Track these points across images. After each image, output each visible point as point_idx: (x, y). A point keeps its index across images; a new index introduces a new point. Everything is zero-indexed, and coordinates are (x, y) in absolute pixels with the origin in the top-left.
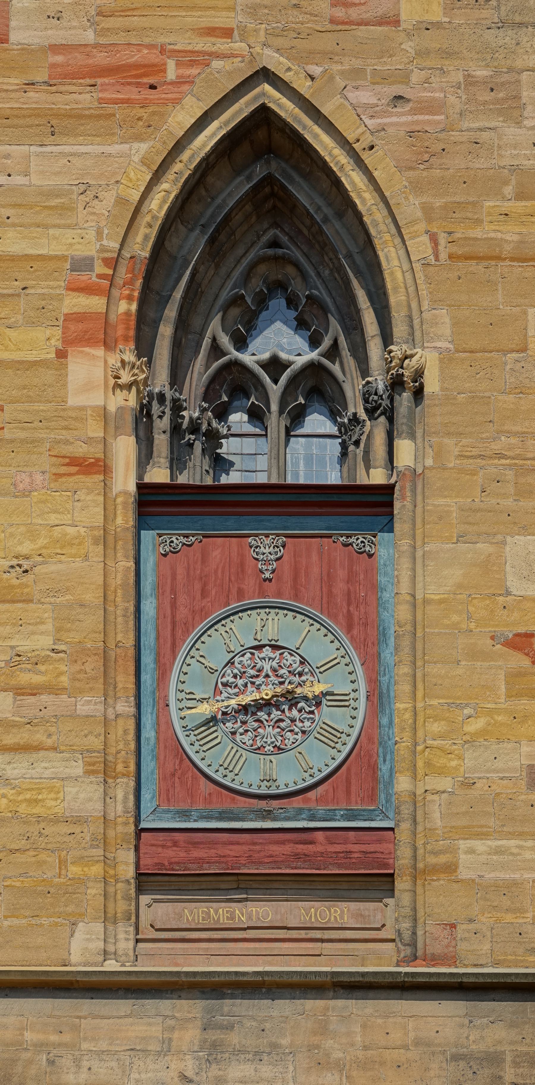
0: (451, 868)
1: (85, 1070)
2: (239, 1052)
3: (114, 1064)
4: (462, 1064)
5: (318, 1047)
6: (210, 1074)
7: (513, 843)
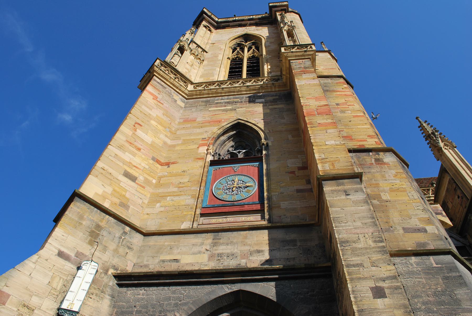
0: (279, 207)
2: (223, 244)
3: (188, 248)
5: (244, 241)
7: (294, 201)
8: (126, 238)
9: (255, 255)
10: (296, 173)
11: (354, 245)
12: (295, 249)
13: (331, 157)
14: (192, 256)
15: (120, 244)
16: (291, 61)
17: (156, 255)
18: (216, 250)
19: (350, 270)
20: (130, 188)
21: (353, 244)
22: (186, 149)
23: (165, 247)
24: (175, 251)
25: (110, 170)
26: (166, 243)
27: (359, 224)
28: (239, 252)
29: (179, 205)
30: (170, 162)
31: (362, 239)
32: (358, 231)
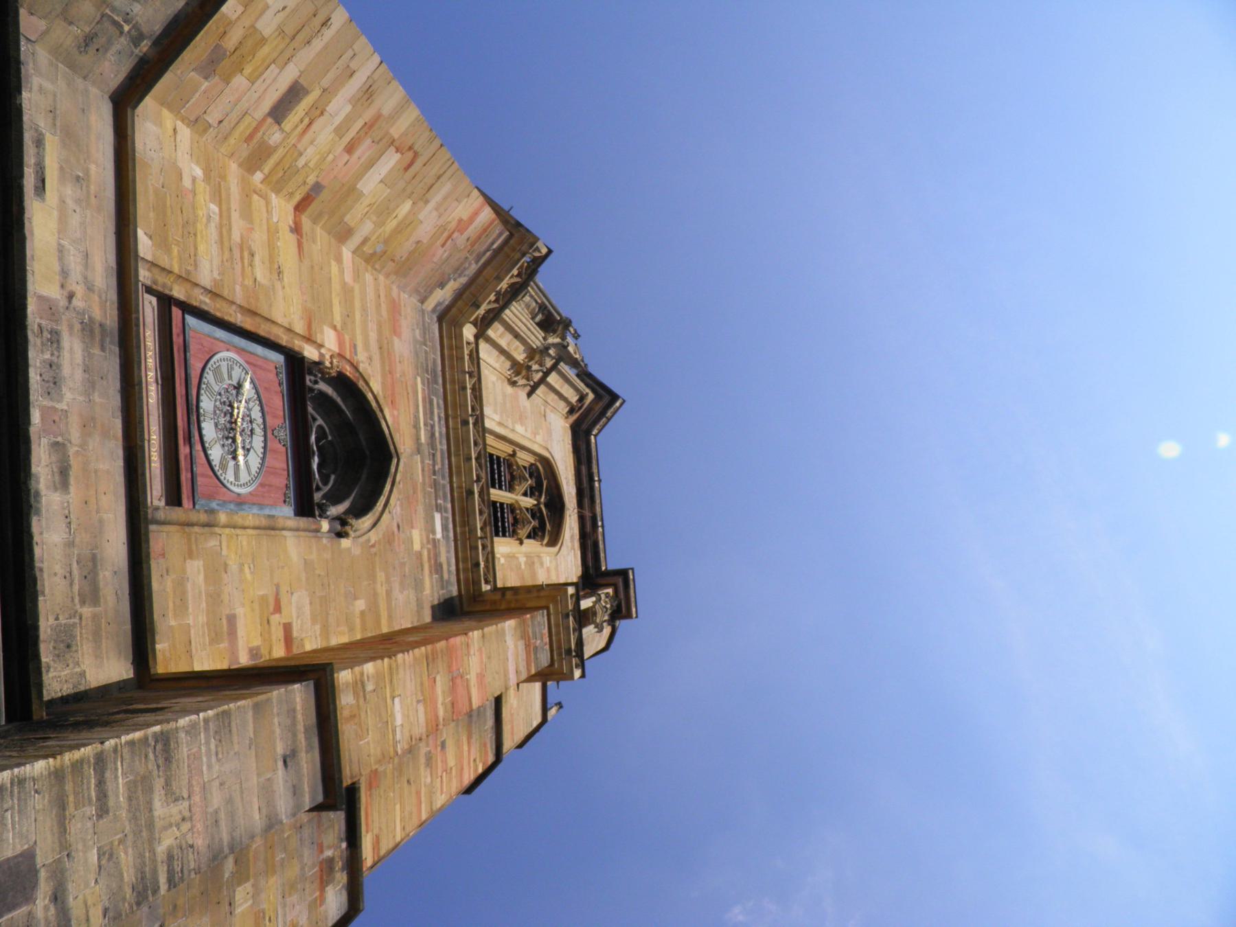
0: (191, 555)
1: (75, 208)
4: (90, 564)
6: (74, 320)
8: (122, 39)
9: (54, 459)
10: (277, 616)
11: (158, 784)
12: (73, 599)
13: (369, 713)
14: (55, 245)
15: (107, 11)
16: (545, 612)
17: (58, 124)
18: (71, 327)
19: (89, 768)
20: (257, 95)
21: (162, 780)
22: (331, 293)
23: (82, 162)
24: (69, 191)
25: (318, 44)
26: (93, 167)
27: (216, 800)
28: (62, 406)
29: (195, 235)
30: (301, 236)
31: (175, 810)
32: (197, 798)
